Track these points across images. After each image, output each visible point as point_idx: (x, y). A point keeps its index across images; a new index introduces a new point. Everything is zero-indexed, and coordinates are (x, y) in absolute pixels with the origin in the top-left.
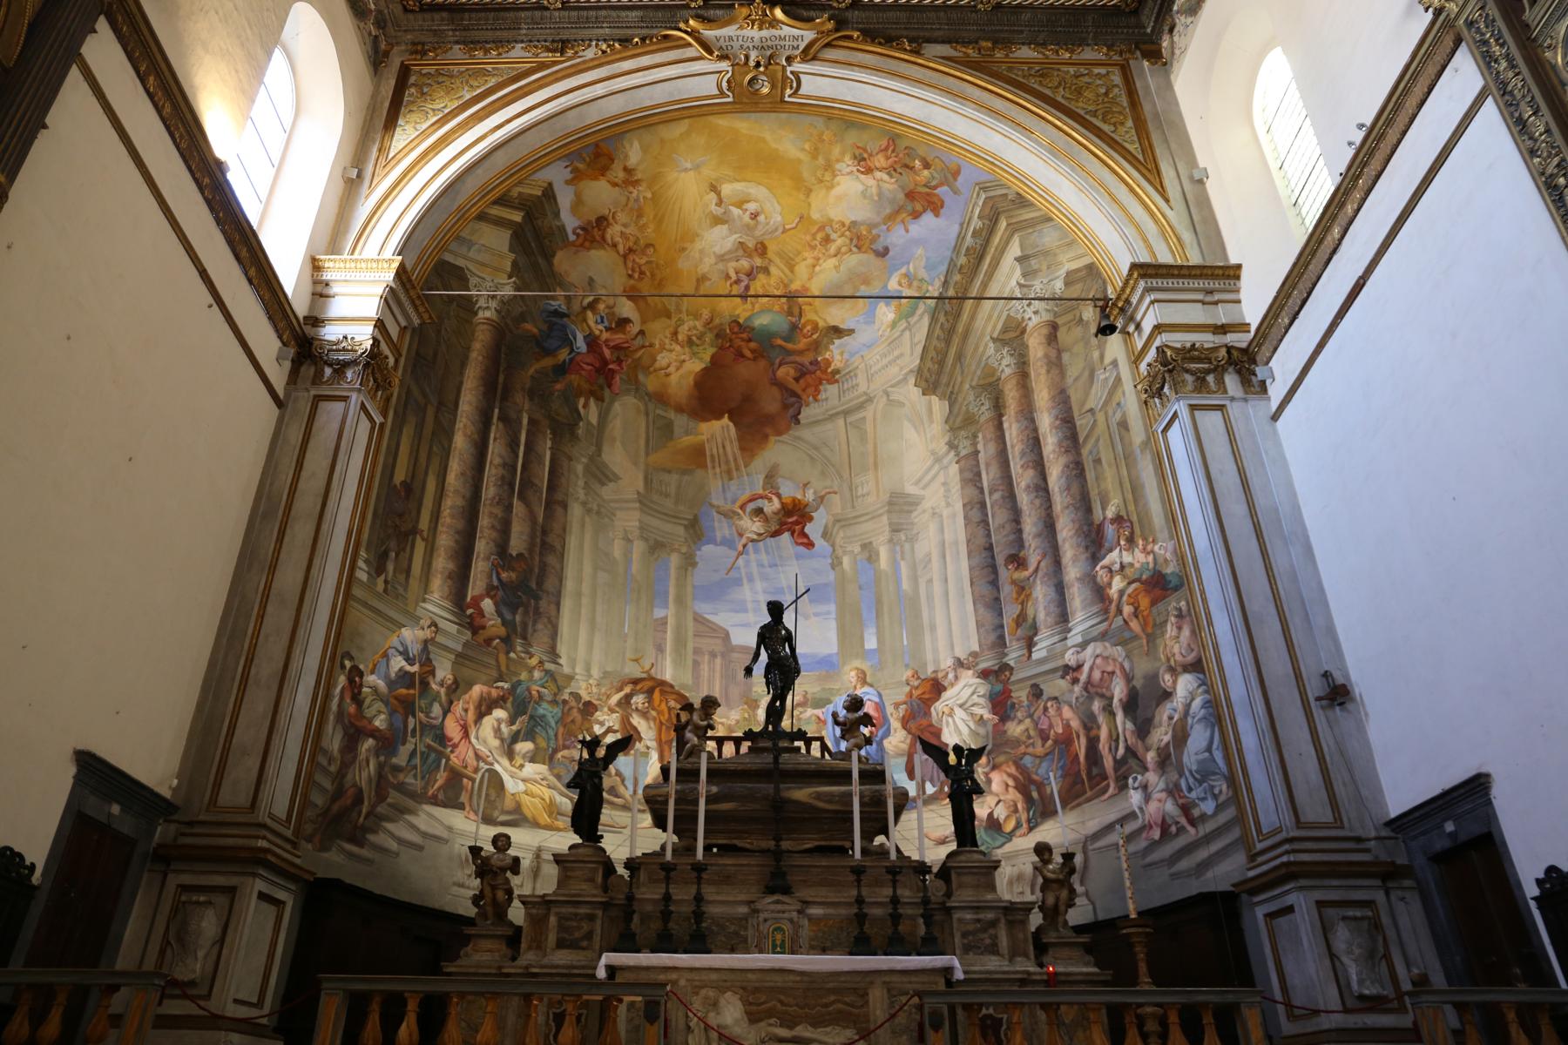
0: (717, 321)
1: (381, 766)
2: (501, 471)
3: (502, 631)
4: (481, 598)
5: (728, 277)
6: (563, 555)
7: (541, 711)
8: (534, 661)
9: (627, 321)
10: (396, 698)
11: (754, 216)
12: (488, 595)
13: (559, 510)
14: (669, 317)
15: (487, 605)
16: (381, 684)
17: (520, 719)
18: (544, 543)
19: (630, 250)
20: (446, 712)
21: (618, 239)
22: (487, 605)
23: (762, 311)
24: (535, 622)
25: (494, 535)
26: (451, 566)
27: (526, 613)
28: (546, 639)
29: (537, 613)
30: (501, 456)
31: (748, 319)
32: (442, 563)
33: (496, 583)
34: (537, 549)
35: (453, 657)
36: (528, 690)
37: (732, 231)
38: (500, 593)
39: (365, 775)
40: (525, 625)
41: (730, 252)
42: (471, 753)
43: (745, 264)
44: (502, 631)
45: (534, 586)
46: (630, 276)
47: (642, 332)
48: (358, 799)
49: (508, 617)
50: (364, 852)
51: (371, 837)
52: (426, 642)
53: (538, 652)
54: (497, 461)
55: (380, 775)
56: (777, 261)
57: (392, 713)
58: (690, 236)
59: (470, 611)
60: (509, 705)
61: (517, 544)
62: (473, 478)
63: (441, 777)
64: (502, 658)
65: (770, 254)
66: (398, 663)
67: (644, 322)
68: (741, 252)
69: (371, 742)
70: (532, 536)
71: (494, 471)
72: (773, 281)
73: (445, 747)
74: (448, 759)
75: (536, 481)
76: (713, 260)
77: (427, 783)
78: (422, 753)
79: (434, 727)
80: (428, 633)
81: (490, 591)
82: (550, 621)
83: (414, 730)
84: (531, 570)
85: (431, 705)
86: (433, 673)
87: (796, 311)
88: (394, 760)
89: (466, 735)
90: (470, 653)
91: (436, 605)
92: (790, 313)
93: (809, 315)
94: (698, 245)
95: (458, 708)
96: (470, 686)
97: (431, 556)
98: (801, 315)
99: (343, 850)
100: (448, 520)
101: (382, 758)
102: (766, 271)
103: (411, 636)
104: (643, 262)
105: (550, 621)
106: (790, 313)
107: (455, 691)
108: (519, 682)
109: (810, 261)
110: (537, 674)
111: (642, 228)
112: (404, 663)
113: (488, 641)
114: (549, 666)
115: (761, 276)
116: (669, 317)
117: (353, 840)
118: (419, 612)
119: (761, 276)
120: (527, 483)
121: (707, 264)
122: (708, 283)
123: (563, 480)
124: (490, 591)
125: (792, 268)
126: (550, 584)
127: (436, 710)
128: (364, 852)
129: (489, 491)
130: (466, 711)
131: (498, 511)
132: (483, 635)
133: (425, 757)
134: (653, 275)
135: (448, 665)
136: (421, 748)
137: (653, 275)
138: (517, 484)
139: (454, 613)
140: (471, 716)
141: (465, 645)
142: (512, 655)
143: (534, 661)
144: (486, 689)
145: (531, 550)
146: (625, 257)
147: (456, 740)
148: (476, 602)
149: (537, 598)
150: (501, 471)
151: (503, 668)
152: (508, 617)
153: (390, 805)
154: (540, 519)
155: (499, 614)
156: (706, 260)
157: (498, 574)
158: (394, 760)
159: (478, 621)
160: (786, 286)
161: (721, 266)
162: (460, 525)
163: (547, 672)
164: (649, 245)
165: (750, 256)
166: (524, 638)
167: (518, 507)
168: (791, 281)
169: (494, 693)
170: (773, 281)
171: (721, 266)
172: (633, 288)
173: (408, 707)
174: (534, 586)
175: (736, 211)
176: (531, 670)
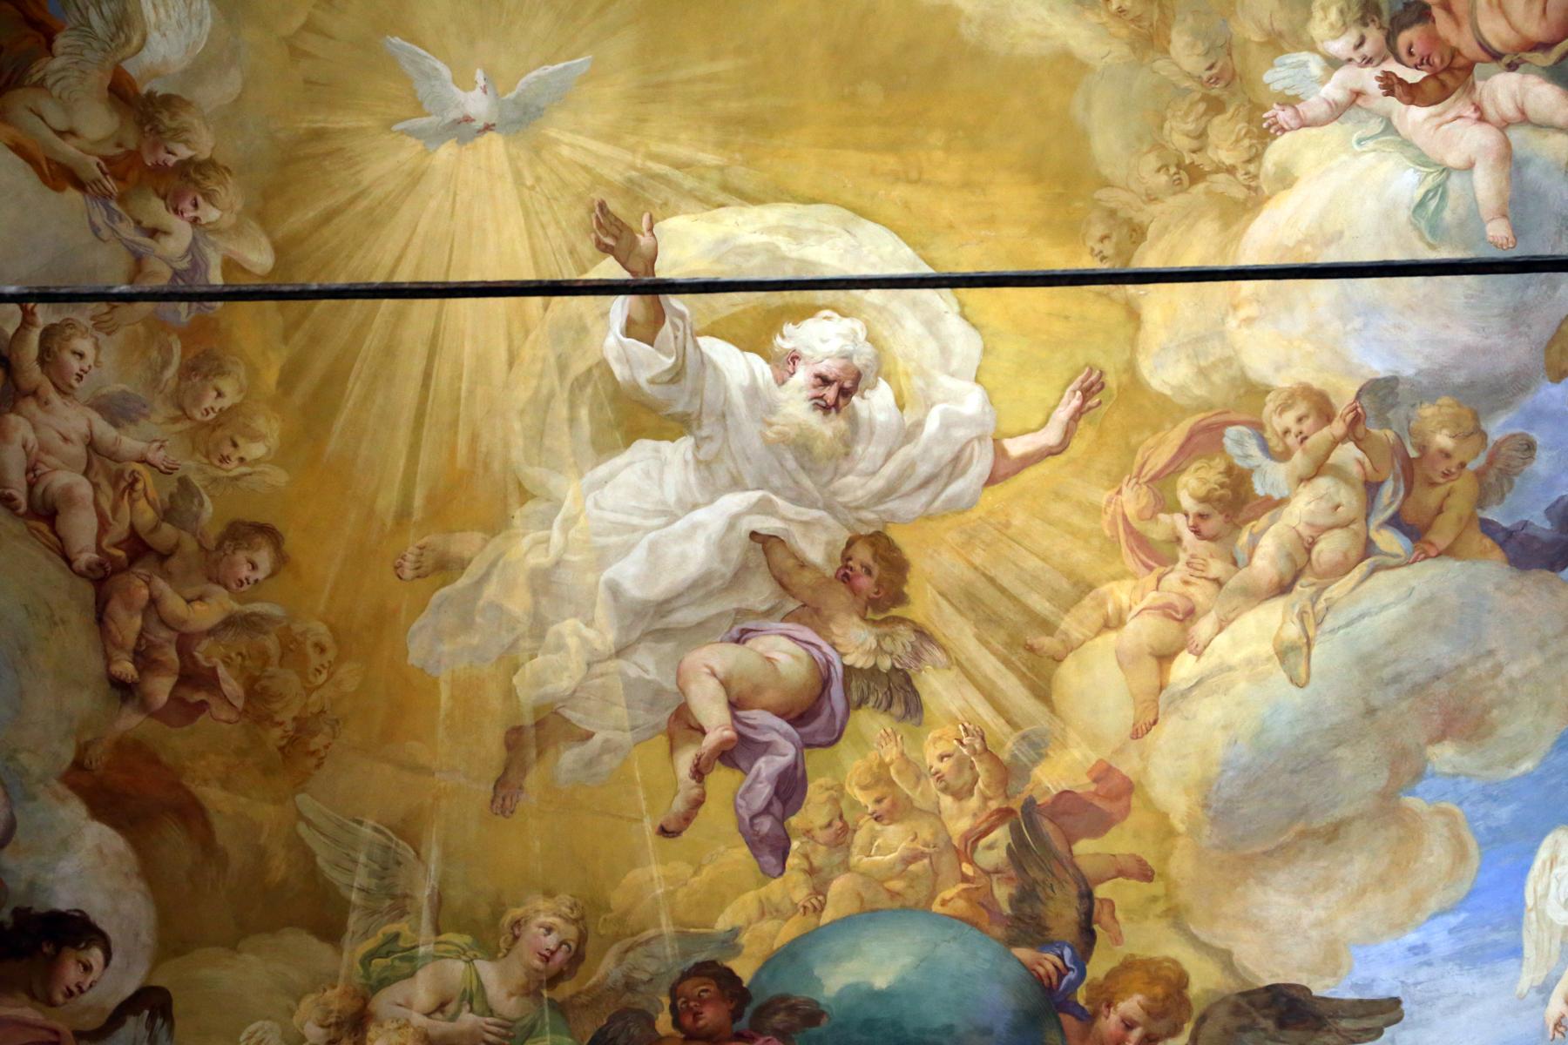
0: (605, 968)
5: (684, 724)
9: (75, 930)
11: (838, 391)
14: (331, 931)
19: (138, 547)
21: (66, 478)
23: (867, 915)
31: (790, 955)
37: (714, 476)
41: (701, 588)
43: (783, 654)
46: (124, 690)
47: (152, 1003)
56: (961, 633)
58: (486, 497)
65: (923, 602)
67: (174, 940)
68: (760, 593)
72: (934, 749)
76: (605, 634)
87: (1062, 913)
92: (1026, 926)
93: (1138, 934)
94: (528, 548)
98: (1087, 935)
102: (898, 692)
104: (206, 614)
106: (1026, 926)
109: (1142, 629)
111: (214, 436)
115: (871, 724)
116: (331, 931)
119: (871, 724)
121: (570, 656)
122: (569, 758)
125: (1039, 671)
134: (256, 692)
137: (256, 692)
146: (102, 581)
156: (568, 628)
160: (1007, 774)
161: (647, 664)
164: (243, 533)
165: (811, 613)
168: (1038, 747)
170: (934, 749)
171: (647, 664)
172: (131, 750)
175: (736, 366)
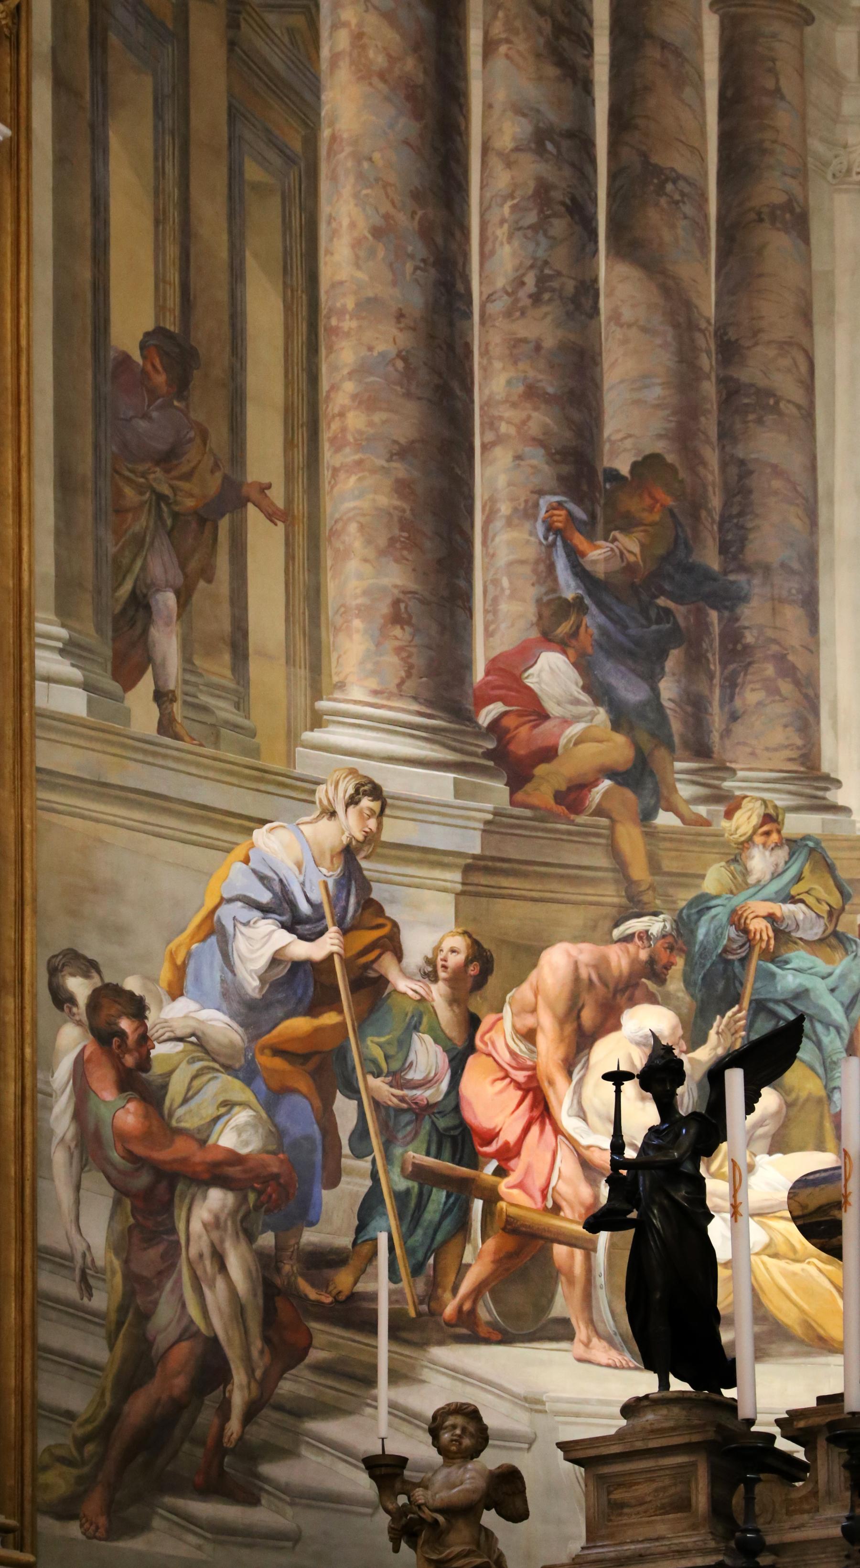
1: (267, 1266)
2: (531, 168)
3: (618, 749)
4: (525, 655)
6: (808, 415)
7: (788, 981)
8: (745, 821)
10: (278, 1051)
12: (548, 639)
13: (777, 243)
15: (552, 675)
16: (219, 1024)
17: (719, 1023)
18: (731, 391)
20: (458, 1060)
22: (552, 675)
24: (731, 686)
25: (540, 419)
26: (396, 577)
27: (696, 662)
28: (779, 736)
29: (736, 651)
30: (519, 110)
32: (362, 576)
33: (569, 587)
34: (710, 425)
35: (455, 877)
36: (737, 920)
38: (593, 621)
39: (217, 1297)
40: (695, 706)
42: (567, 1164)
44: (618, 749)
45: (711, 559)
48: (212, 1369)
49: (632, 692)
50: (262, 1516)
51: (276, 1471)
52: (348, 853)
53: (755, 785)
54: (511, 132)
55: (271, 1289)
57: (273, 1099)
59: (487, 715)
60: (675, 985)
61: (629, 428)
62: (425, 232)
63: (478, 1256)
64: (630, 837)
66: (261, 944)
69: (216, 1199)
70: (686, 378)
71: (503, 179)
73: (474, 1162)
74: (492, 1198)
75: (677, 161)
77: (434, 1284)
78: (401, 1198)
79: (429, 1108)
80: (351, 825)
81: (554, 623)
82: (787, 670)
83: (361, 1134)
84: (696, 507)
85: (404, 1044)
86: (392, 944)
88: (310, 1237)
89: (541, 1110)
90: (512, 850)
91: (363, 722)
95: (500, 1035)
96: (529, 954)
97: (315, 564)
99: (190, 1521)
100: (356, 421)
101: (267, 1239)
103: (294, 848)
105: (787, 670)
107: (480, 982)
108: (702, 905)
110: (760, 862)
112: (283, 938)
113: (572, 797)
114: (798, 824)
117: (217, 1486)
118: (307, 763)
120: (640, 181)
123: (783, 118)
124: (554, 623)
126: (769, 541)
127: (427, 1057)
128: (262, 1516)
129: (497, 259)
130: (529, 1036)
131: (543, 328)
132: (548, 780)
133: (410, 1210)
135: (442, 907)
136: (395, 1181)
138: (601, 196)
139: (433, 735)
140: (549, 1050)
141: (490, 829)
142: (665, 819)
143: (745, 821)
144: (585, 953)
145: (684, 435)
147: (510, 1135)
148: (509, 674)
149: (729, 600)
150: (531, 168)
151: (639, 871)
152: (632, 692)
153: (320, 1368)
154: (708, 306)
155: (598, 691)
157: (574, 557)
158: (310, 1237)
159: (525, 738)
162: (404, 421)
163: (794, 845)
166: (701, 750)
167: (618, 285)
169: (619, 959)
173: (328, 1068)
174: (711, 559)
176: (736, 855)
